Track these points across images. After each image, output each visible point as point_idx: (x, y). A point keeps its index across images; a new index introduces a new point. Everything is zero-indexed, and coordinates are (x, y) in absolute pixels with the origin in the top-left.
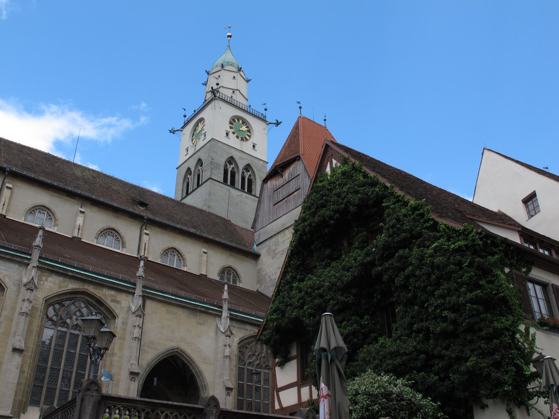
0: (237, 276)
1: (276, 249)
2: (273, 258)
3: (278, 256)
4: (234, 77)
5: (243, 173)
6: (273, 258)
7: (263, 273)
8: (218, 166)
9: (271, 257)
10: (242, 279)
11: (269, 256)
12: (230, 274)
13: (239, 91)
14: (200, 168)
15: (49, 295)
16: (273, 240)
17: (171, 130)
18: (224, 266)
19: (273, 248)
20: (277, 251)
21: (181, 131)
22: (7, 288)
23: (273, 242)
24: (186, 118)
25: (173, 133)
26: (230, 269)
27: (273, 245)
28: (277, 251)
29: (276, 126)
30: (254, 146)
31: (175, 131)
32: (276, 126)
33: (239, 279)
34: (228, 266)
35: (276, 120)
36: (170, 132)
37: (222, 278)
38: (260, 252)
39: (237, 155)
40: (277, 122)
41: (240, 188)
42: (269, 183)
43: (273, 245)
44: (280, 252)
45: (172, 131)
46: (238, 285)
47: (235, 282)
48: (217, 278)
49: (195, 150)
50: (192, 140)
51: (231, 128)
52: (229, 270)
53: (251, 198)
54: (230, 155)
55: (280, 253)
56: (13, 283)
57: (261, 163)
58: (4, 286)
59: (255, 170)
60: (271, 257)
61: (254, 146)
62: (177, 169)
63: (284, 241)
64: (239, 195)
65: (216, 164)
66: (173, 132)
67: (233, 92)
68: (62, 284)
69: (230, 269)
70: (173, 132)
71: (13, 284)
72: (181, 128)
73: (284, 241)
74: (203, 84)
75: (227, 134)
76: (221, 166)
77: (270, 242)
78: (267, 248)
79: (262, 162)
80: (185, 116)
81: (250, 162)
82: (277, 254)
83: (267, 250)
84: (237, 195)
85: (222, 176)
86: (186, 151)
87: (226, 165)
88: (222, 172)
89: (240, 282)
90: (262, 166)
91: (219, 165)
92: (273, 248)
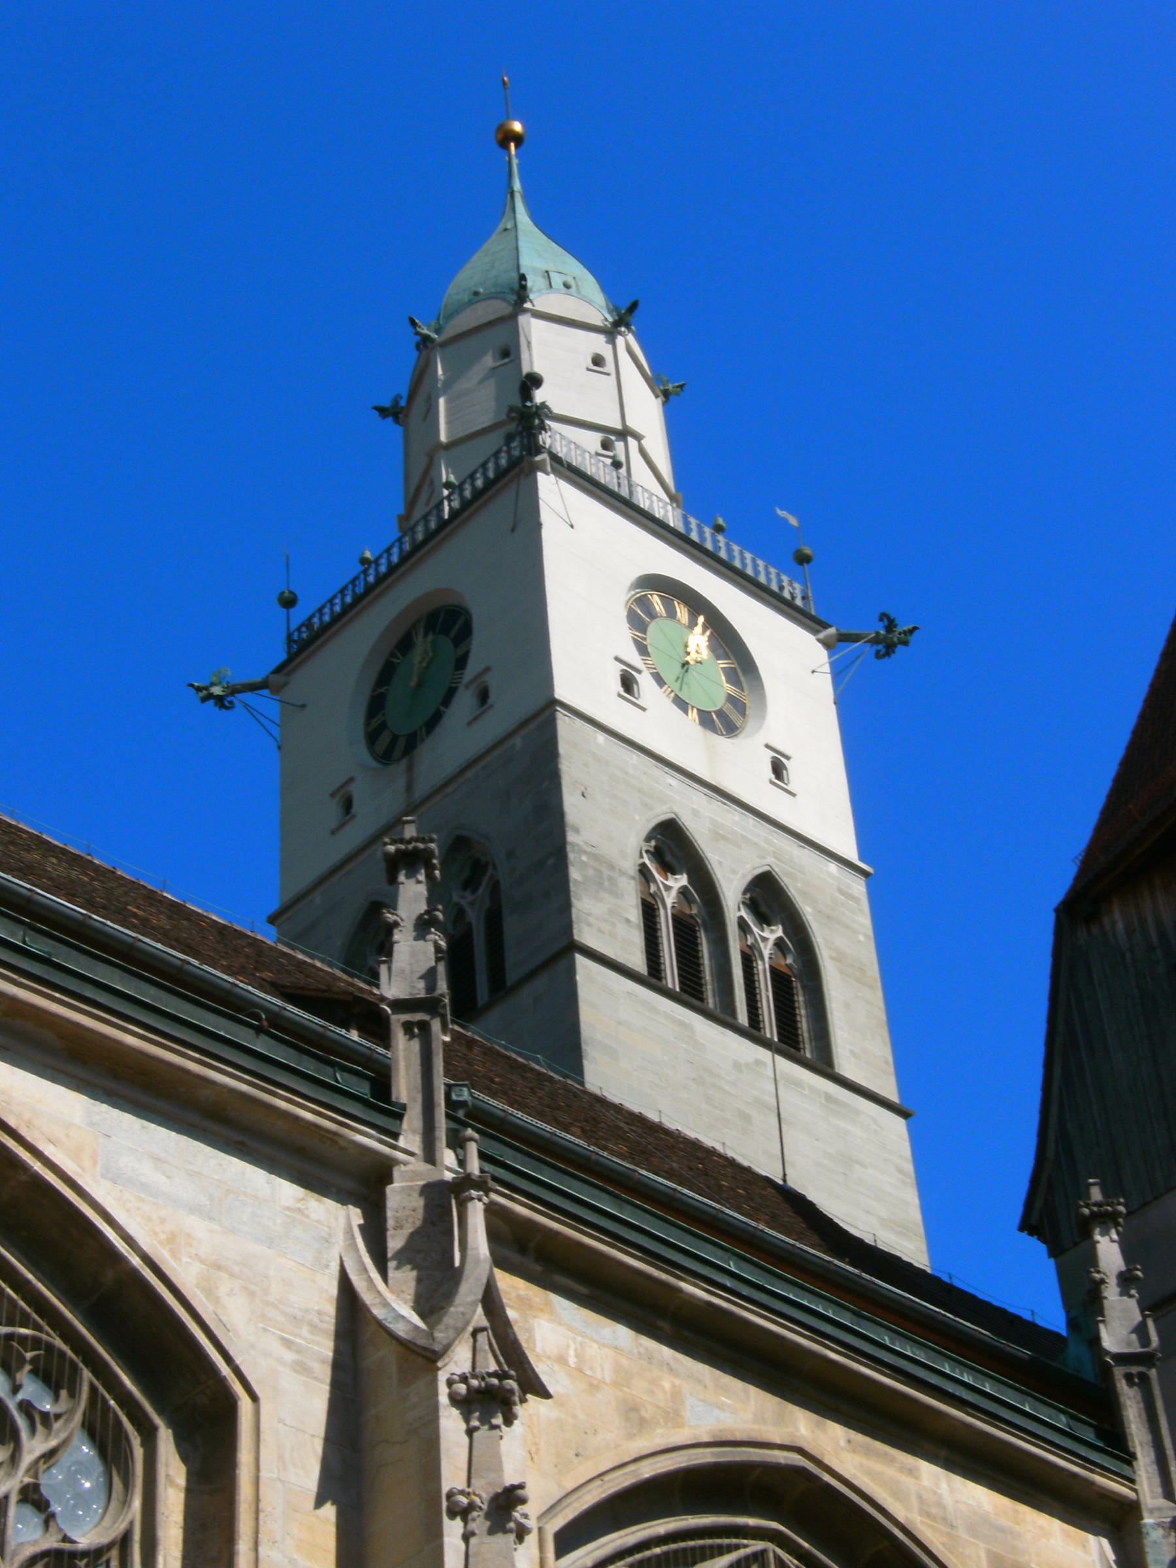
4: (598, 361)
5: (743, 925)
8: (606, 872)
13: (638, 437)
15: (570, 1485)
21: (277, 689)
22: (254, 1398)
24: (299, 615)
25: (220, 701)
29: (878, 656)
30: (778, 769)
32: (878, 656)
35: (883, 616)
36: (204, 700)
39: (695, 813)
40: (891, 626)
41: (743, 1018)
42: (1117, 919)
45: (217, 690)
49: (409, 787)
51: (643, 650)
53: (812, 1089)
54: (661, 814)
56: (288, 1344)
57: (830, 874)
58: (225, 1370)
59: (808, 912)
61: (778, 769)
62: (272, 920)
64: (747, 1065)
65: (595, 857)
67: (606, 445)
68: (639, 1390)
71: (289, 1356)
72: (278, 670)
74: (383, 412)
75: (628, 683)
76: (622, 873)
79: (833, 867)
80: (289, 602)
81: (770, 860)
84: (737, 1066)
85: (637, 938)
86: (333, 810)
87: (643, 871)
88: (635, 915)
90: (840, 891)
91: (612, 867)
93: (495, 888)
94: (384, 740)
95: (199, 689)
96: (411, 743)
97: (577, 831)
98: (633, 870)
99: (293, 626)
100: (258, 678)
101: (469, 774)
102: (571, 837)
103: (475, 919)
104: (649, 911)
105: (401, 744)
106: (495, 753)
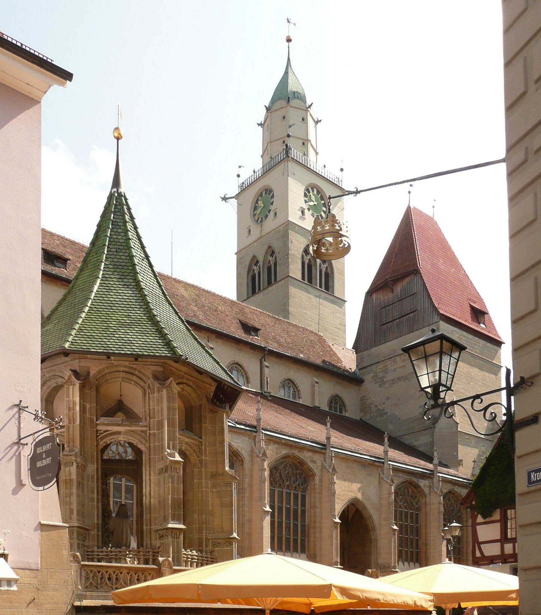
0: (343, 405)
1: (384, 377)
2: (380, 386)
3: (387, 385)
6: (380, 386)
7: (368, 402)
9: (378, 385)
10: (348, 408)
11: (375, 383)
12: (337, 402)
14: (270, 258)
16: (381, 366)
17: (223, 197)
18: (332, 395)
19: (381, 375)
20: (385, 380)
23: (380, 369)
26: (337, 398)
27: (380, 372)
28: (385, 380)
31: (228, 198)
33: (345, 408)
34: (335, 395)
36: (222, 200)
37: (330, 408)
38: (363, 377)
43: (380, 372)
44: (390, 381)
46: (344, 414)
47: (341, 412)
48: (327, 409)
50: (254, 215)
52: (336, 399)
55: (389, 382)
60: (378, 385)
63: (395, 370)
66: (225, 199)
69: (337, 398)
70: (225, 199)
72: (237, 195)
73: (395, 370)
77: (376, 368)
78: (373, 374)
82: (385, 383)
83: (372, 377)
89: (346, 411)
92: (381, 375)
93: (276, 258)
94: (256, 218)
95: (221, 198)
96: (261, 221)
97: (291, 250)
98: (300, 256)
99: (240, 184)
100: (233, 196)
101: (273, 232)
102: (290, 252)
103: (272, 263)
104: (303, 263)
105: (260, 219)
106: (277, 229)
